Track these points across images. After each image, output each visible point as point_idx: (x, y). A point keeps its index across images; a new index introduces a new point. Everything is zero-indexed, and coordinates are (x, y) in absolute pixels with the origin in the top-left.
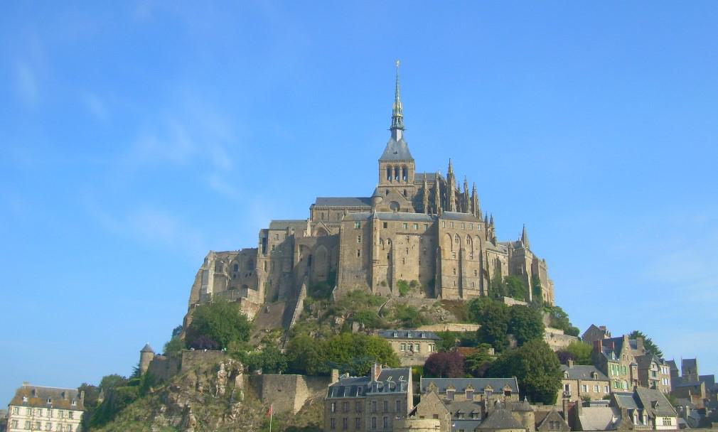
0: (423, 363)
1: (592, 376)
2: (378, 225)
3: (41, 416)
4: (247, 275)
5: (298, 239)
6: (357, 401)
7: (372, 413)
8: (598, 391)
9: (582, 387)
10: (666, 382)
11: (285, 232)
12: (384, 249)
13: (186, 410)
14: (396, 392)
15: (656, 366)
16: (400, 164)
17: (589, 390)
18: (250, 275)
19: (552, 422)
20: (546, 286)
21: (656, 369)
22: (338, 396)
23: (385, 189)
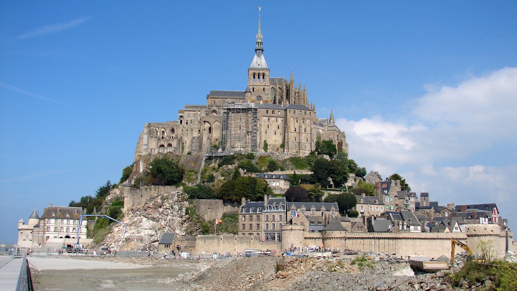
1: (375, 202)
3: (64, 224)
5: (203, 117)
6: (257, 215)
7: (266, 221)
10: (412, 204)
11: (195, 112)
15: (408, 197)
17: (373, 210)
18: (173, 137)
21: (408, 199)
23: (251, 87)
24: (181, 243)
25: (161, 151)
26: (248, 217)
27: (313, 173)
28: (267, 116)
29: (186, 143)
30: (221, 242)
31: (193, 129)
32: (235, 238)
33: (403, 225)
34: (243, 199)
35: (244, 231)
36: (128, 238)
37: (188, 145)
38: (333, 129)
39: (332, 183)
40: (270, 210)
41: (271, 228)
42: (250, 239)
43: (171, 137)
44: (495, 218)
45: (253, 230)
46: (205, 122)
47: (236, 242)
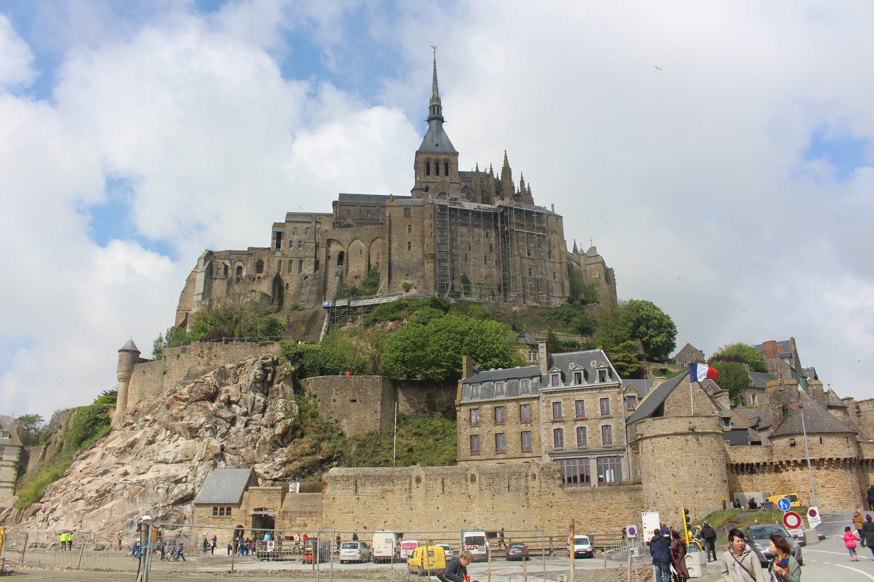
5: (326, 231)
7: (553, 422)
16: (443, 157)
22: (481, 399)
24: (270, 500)
26: (490, 412)
30: (418, 492)
31: (303, 259)
32: (469, 476)
35: (478, 457)
36: (103, 489)
37: (291, 292)
38: (599, 260)
40: (565, 385)
41: (570, 442)
42: (527, 476)
45: (510, 453)
47: (473, 489)
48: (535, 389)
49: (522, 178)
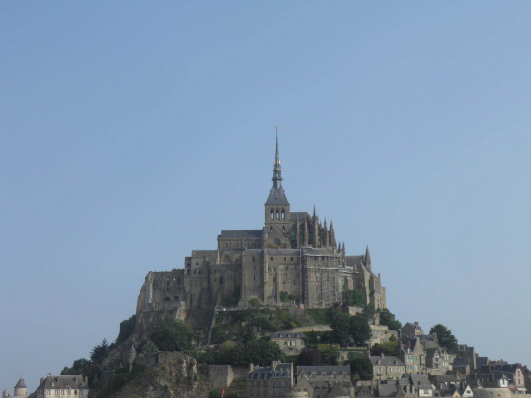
0: (298, 354)
1: (395, 363)
2: (267, 258)
4: (176, 289)
5: (213, 265)
8: (398, 372)
9: (388, 370)
10: (446, 363)
12: (271, 275)
13: (166, 388)
14: (285, 377)
16: (280, 207)
17: (393, 371)
18: (179, 288)
19: (364, 392)
20: (379, 293)
21: (438, 357)
23: (269, 226)
25: (166, 305)
27: (332, 330)
28: (285, 264)
29: (195, 295)
33: (411, 390)
34: (252, 365)
39: (352, 341)
43: (178, 288)
44: (519, 380)
46: (215, 271)
48: (268, 377)
49: (325, 220)
